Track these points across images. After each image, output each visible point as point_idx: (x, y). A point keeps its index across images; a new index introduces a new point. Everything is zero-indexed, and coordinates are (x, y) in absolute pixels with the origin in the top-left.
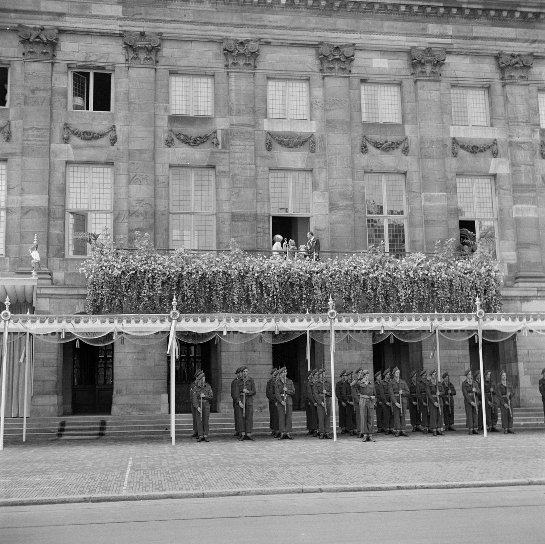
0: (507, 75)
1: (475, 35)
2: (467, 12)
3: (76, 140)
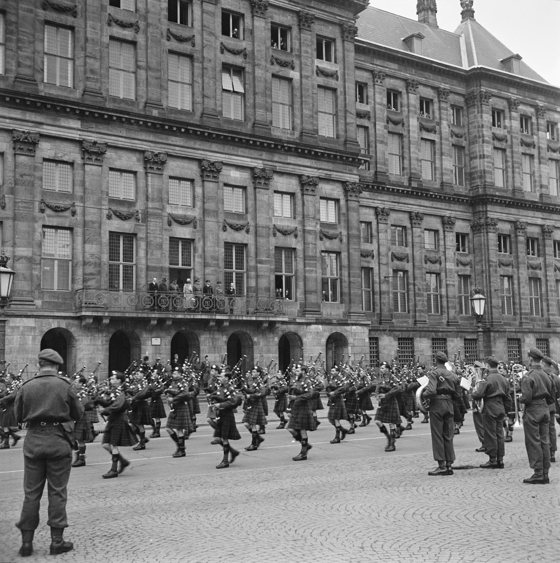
0: (305, 188)
1: (289, 161)
2: (286, 148)
3: (48, 211)
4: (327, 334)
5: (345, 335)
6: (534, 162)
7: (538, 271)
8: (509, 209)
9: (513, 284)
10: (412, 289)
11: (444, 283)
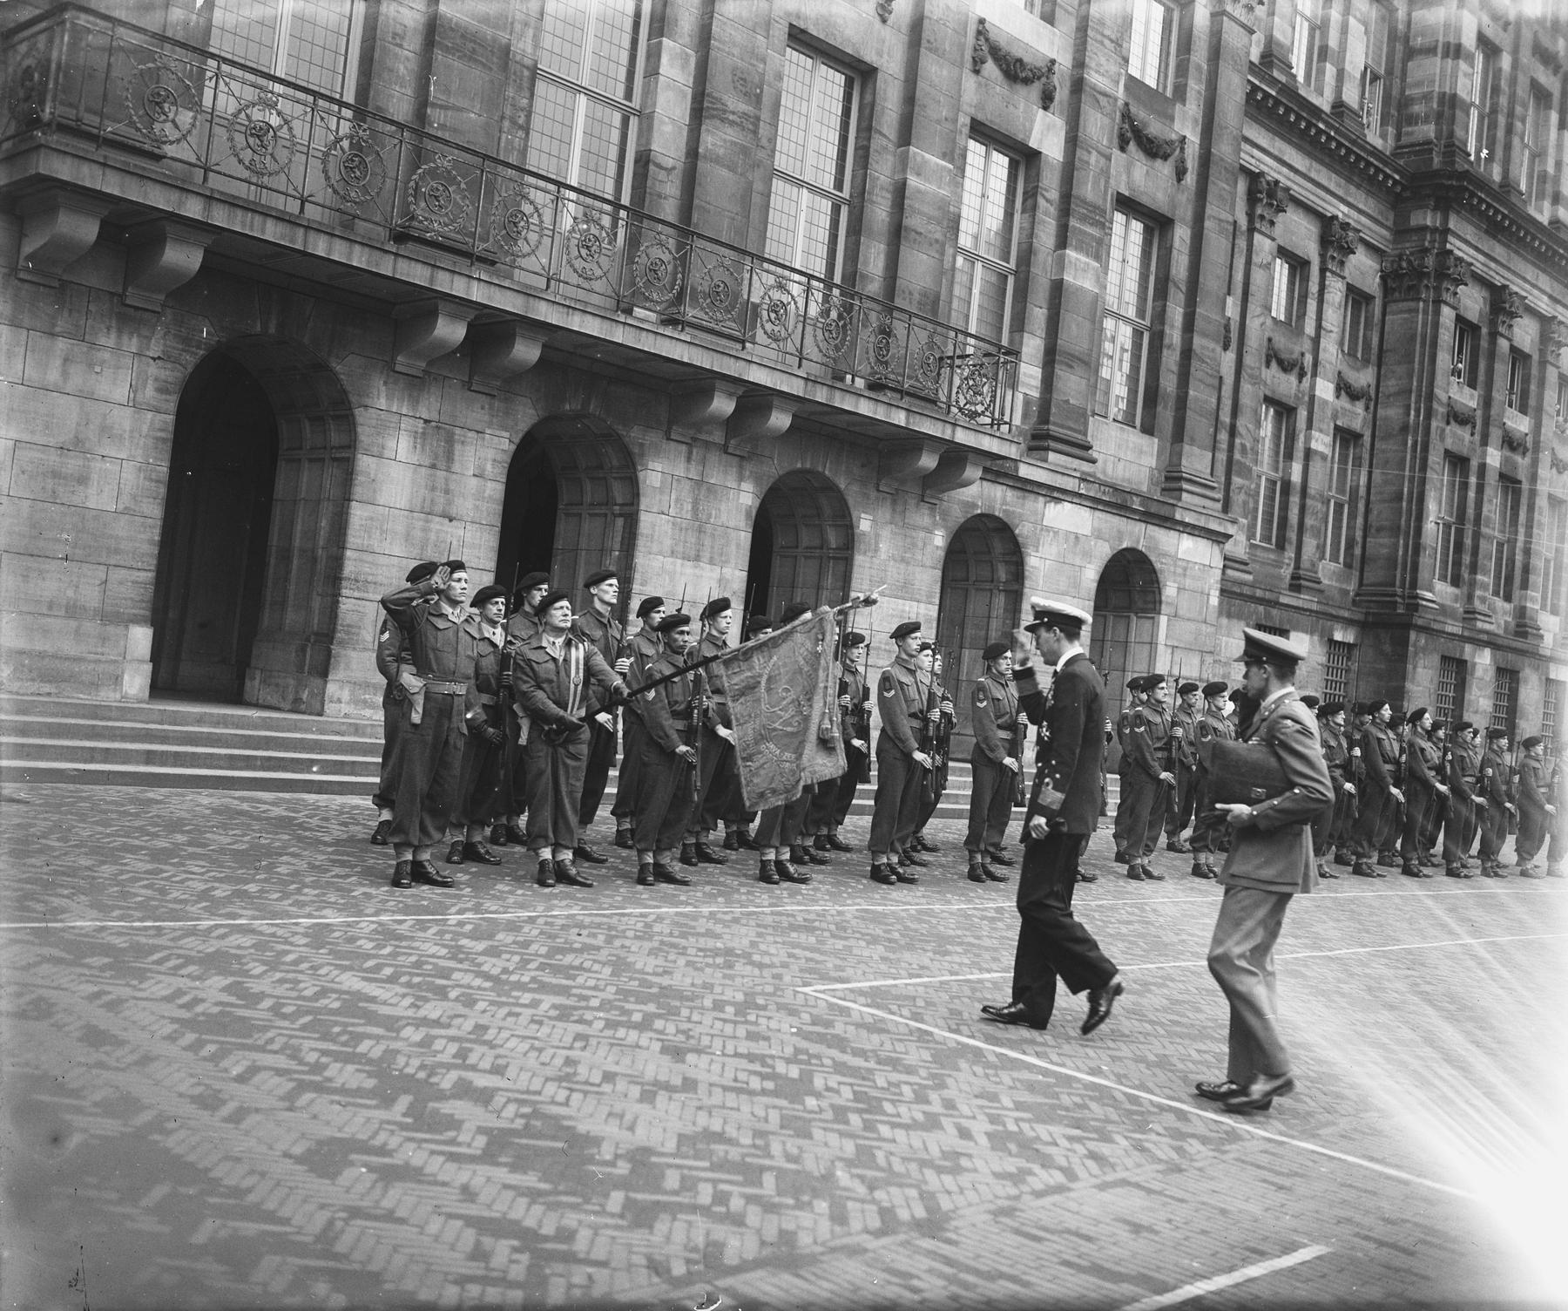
4: (1104, 552)
5: (1158, 566)
6: (1547, 120)
7: (1519, 459)
8: (1492, 242)
9: (1465, 486)
10: (1224, 446)
11: (1300, 444)
